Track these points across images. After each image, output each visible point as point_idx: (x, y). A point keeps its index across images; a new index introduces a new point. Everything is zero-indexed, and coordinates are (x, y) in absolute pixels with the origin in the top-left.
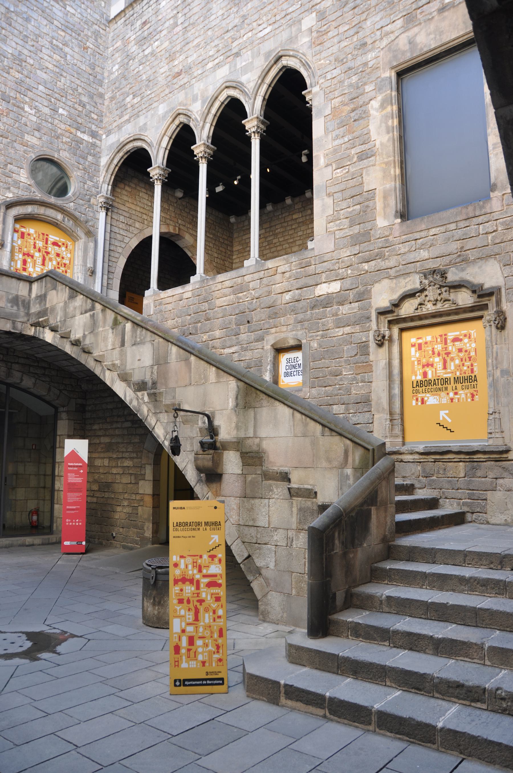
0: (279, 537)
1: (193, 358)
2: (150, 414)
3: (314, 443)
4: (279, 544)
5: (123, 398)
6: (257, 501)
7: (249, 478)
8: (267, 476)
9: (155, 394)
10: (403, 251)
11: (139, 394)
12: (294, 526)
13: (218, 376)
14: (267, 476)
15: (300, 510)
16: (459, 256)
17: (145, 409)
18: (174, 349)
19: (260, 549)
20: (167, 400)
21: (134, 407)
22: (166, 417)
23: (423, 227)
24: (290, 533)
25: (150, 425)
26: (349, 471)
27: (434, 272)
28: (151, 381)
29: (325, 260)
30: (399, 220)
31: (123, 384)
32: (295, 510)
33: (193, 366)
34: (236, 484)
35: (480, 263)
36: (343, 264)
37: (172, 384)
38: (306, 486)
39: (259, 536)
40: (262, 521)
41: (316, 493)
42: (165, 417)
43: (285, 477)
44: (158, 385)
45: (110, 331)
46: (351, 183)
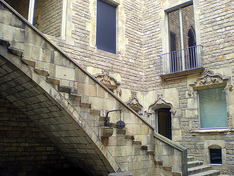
0: (129, 159)
1: (97, 85)
2: (70, 106)
3: (141, 127)
4: (129, 161)
5: (48, 93)
6: (122, 147)
7: (119, 138)
8: (127, 137)
9: (75, 96)
10: (96, 59)
11: (62, 94)
12: (134, 154)
13: (109, 97)
14: (127, 137)
15: (135, 149)
16: (112, 69)
17: (66, 103)
18: (87, 78)
19: (123, 165)
20: (84, 101)
21: (58, 100)
22: (80, 109)
23: (103, 54)
24: (133, 157)
25: (70, 111)
26: (149, 135)
27: (105, 70)
28: (73, 89)
29: (70, 48)
30: (96, 48)
31: (48, 85)
32: (134, 149)
33: (97, 89)
34: (114, 141)
35: (117, 73)
36: (77, 53)
37: (87, 93)
38: (139, 141)
39: (122, 160)
40: (124, 154)
41: (141, 143)
42: (78, 109)
43: (132, 138)
44: (78, 92)
45: (41, 50)
46: (82, 24)
